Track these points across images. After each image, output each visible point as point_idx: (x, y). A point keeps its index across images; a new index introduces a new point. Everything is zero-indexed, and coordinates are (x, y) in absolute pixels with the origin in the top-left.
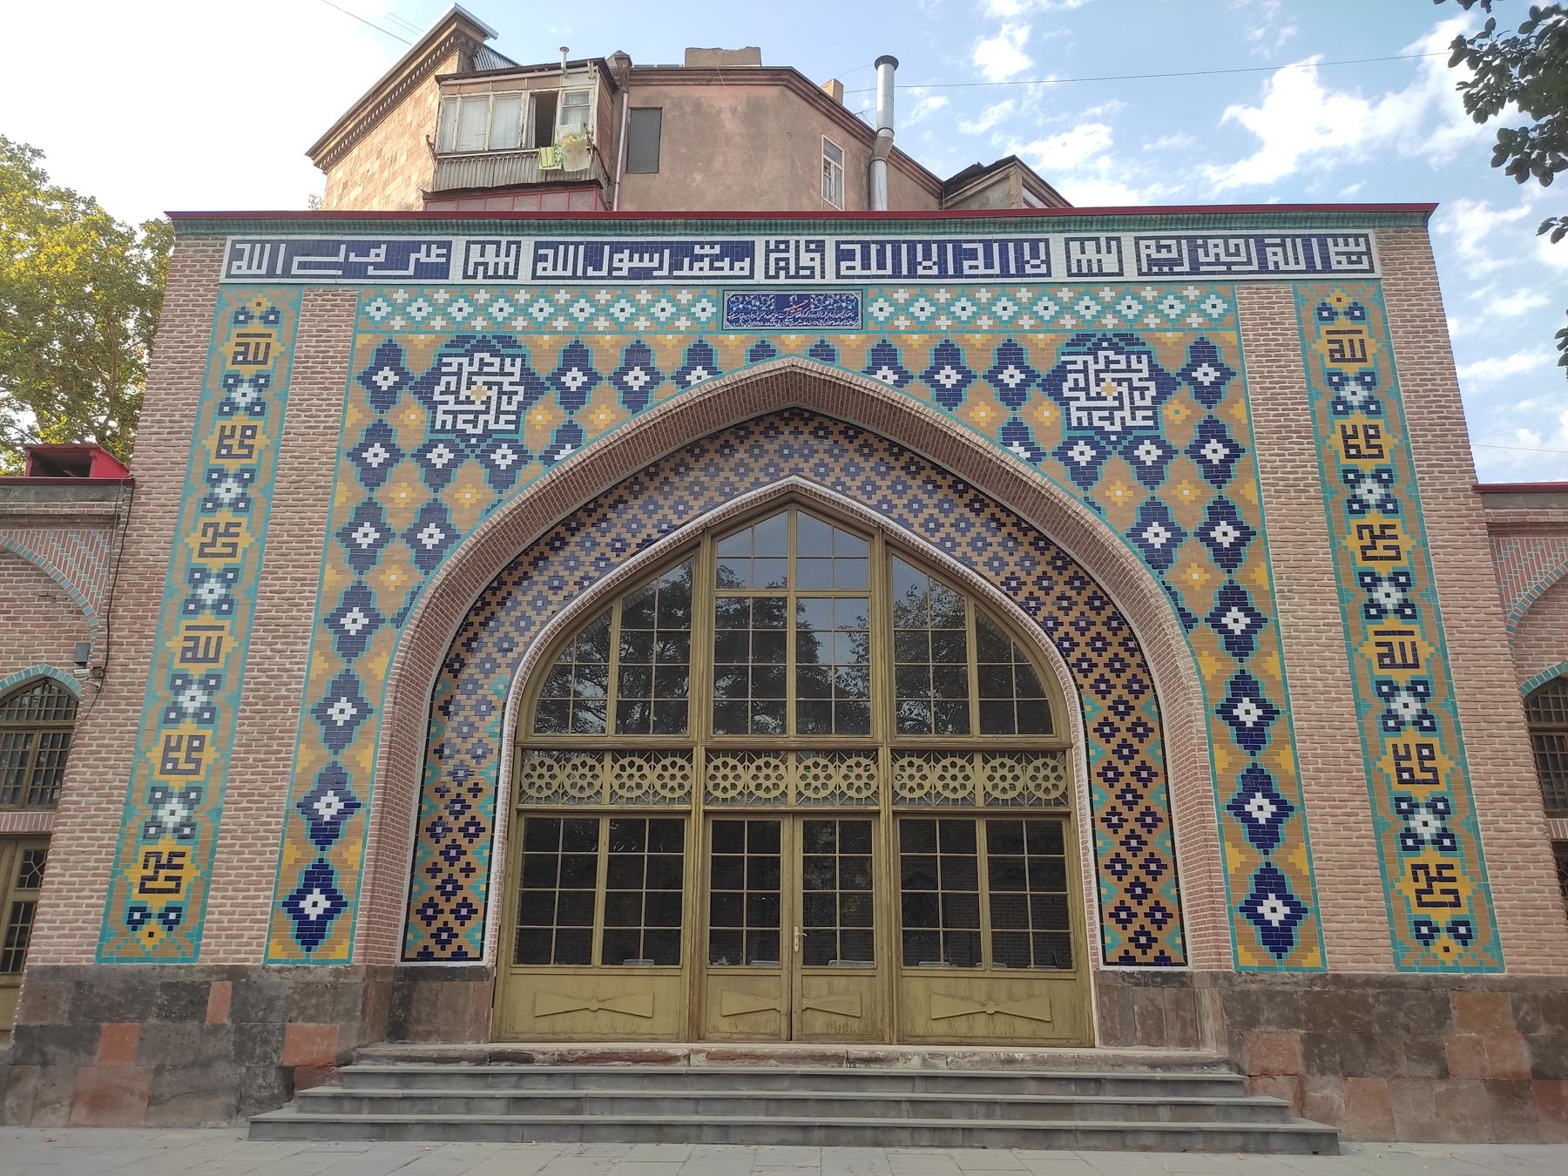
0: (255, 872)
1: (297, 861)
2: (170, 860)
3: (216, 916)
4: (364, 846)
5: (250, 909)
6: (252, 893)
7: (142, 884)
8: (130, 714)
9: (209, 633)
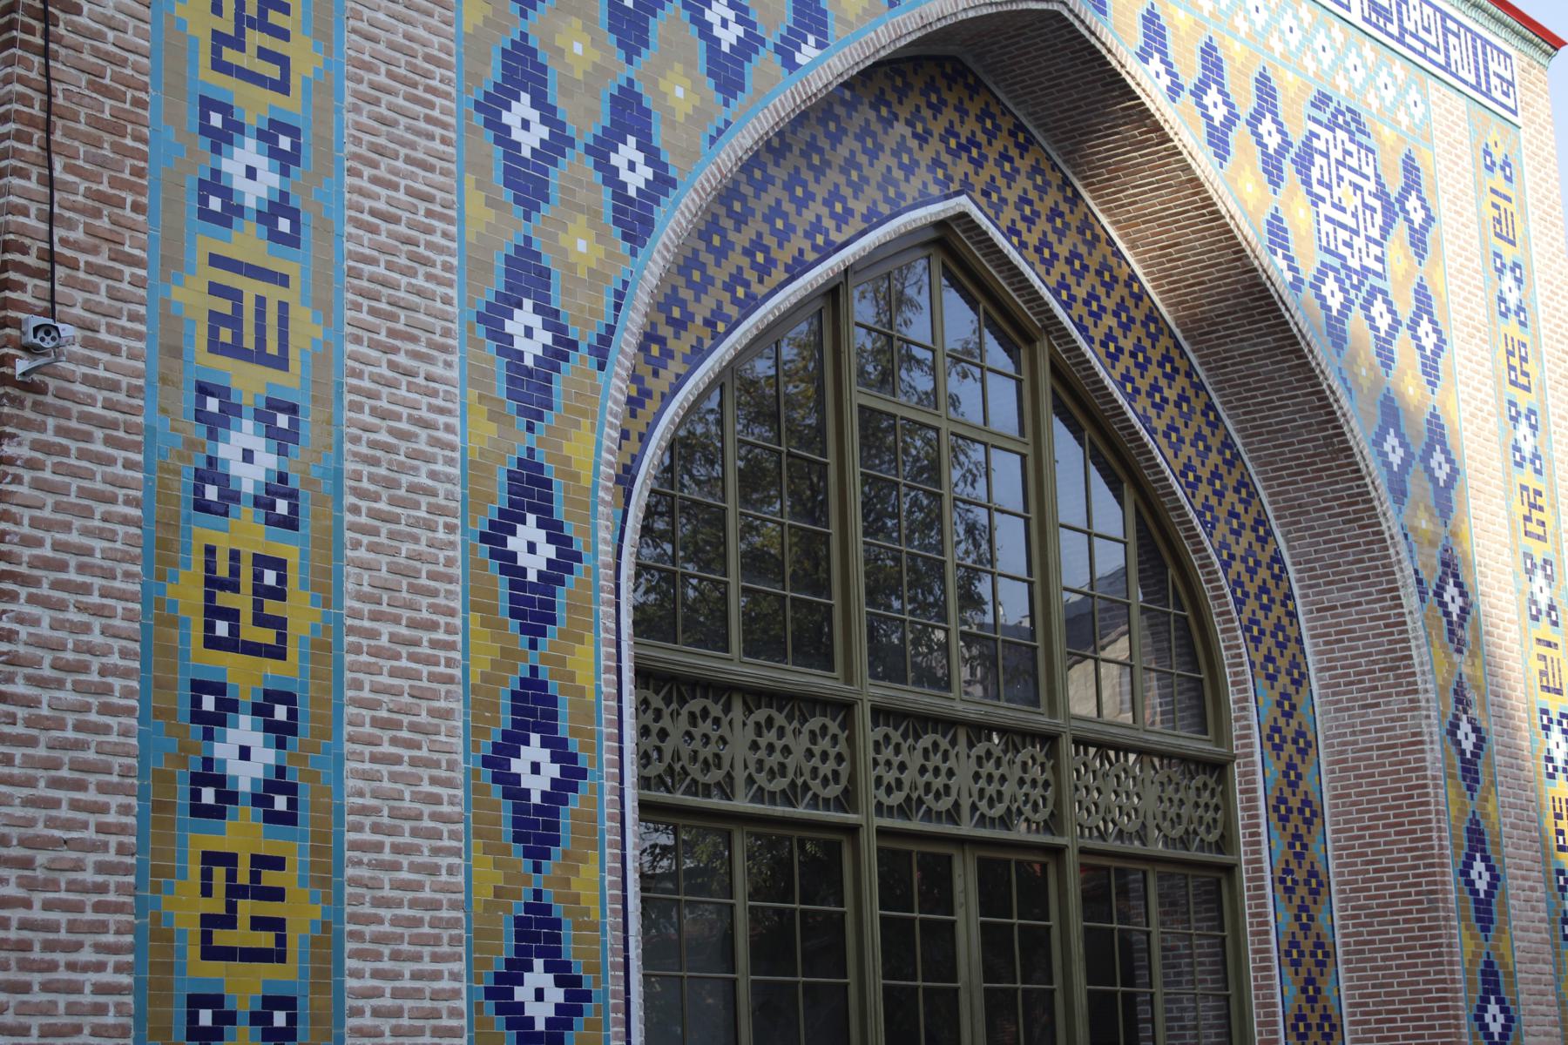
0: (427, 916)
1: (498, 892)
2: (255, 877)
3: (367, 1021)
4: (602, 870)
5: (427, 1004)
6: (427, 965)
7: (206, 937)
8: (119, 470)
9: (263, 288)
